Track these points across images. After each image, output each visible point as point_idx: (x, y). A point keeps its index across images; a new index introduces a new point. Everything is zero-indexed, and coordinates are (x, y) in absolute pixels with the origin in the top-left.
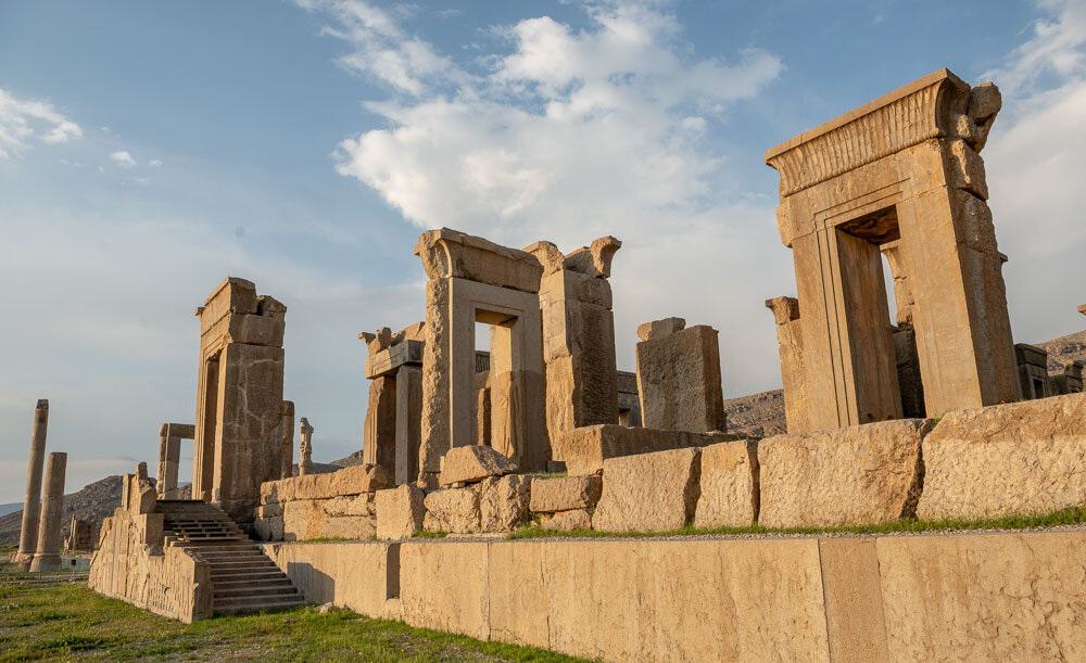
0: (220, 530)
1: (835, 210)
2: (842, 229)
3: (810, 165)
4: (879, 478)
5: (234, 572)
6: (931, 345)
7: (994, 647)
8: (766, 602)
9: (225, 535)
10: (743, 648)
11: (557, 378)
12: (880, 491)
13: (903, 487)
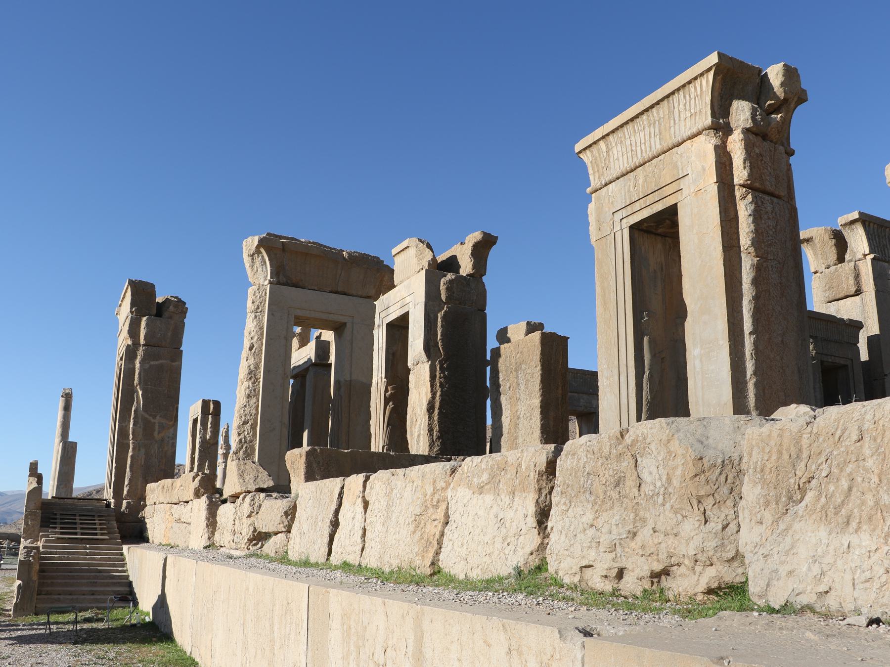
3: (612, 159)
6: (697, 362)
11: (417, 386)
12: (421, 538)
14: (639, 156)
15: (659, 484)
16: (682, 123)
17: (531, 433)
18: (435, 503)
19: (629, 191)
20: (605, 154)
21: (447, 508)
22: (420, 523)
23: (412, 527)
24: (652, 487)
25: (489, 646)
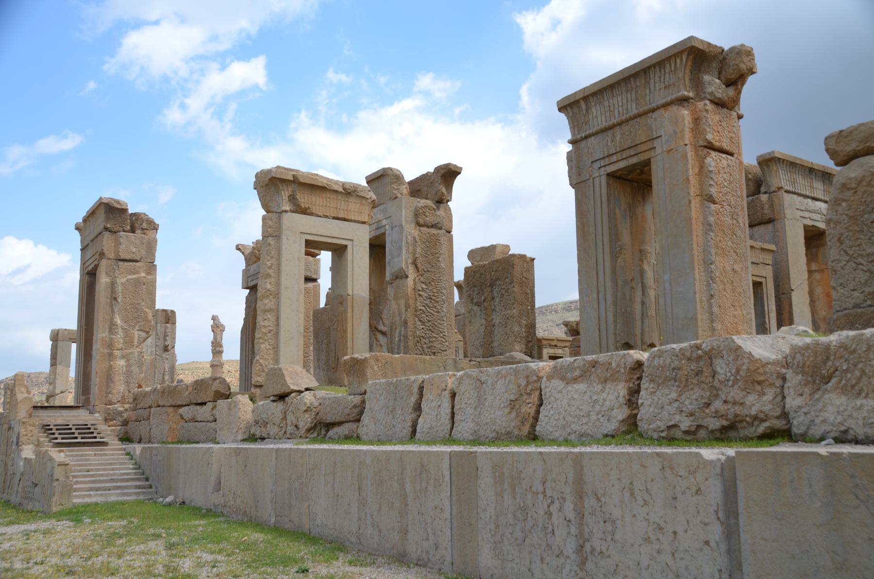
0: (92, 433)
1: (607, 159)
2: (614, 177)
3: (591, 117)
4: (517, 406)
5: (98, 470)
7: (525, 526)
8: (423, 494)
9: (95, 437)
10: (410, 527)
12: (517, 416)
13: (529, 414)
14: (617, 116)
15: (729, 374)
16: (656, 94)
17: (506, 337)
18: (529, 392)
19: (607, 145)
20: (584, 112)
21: (541, 395)
22: (515, 406)
23: (507, 410)
24: (724, 376)
25: (645, 467)
